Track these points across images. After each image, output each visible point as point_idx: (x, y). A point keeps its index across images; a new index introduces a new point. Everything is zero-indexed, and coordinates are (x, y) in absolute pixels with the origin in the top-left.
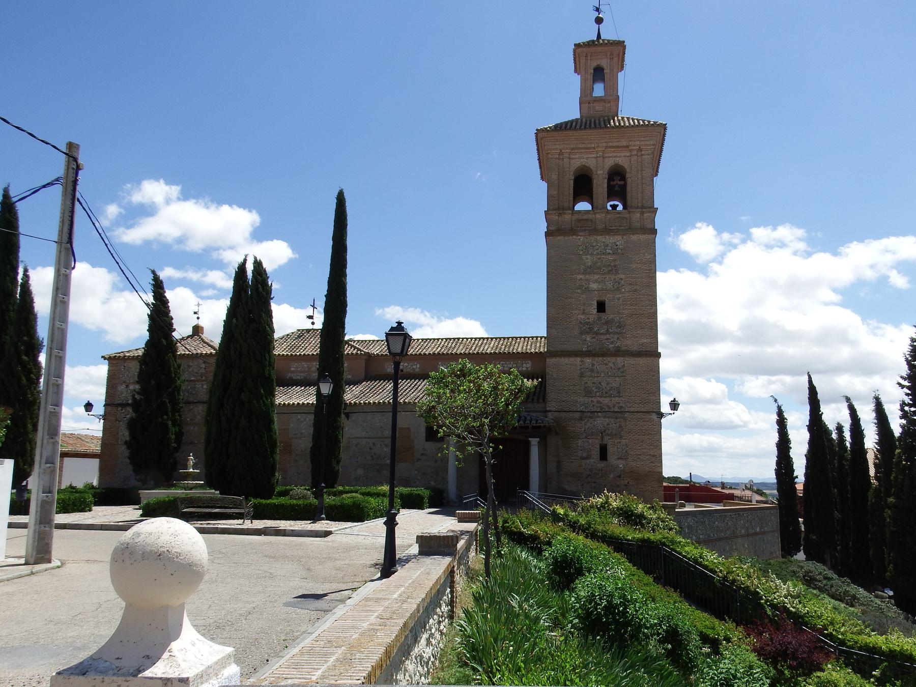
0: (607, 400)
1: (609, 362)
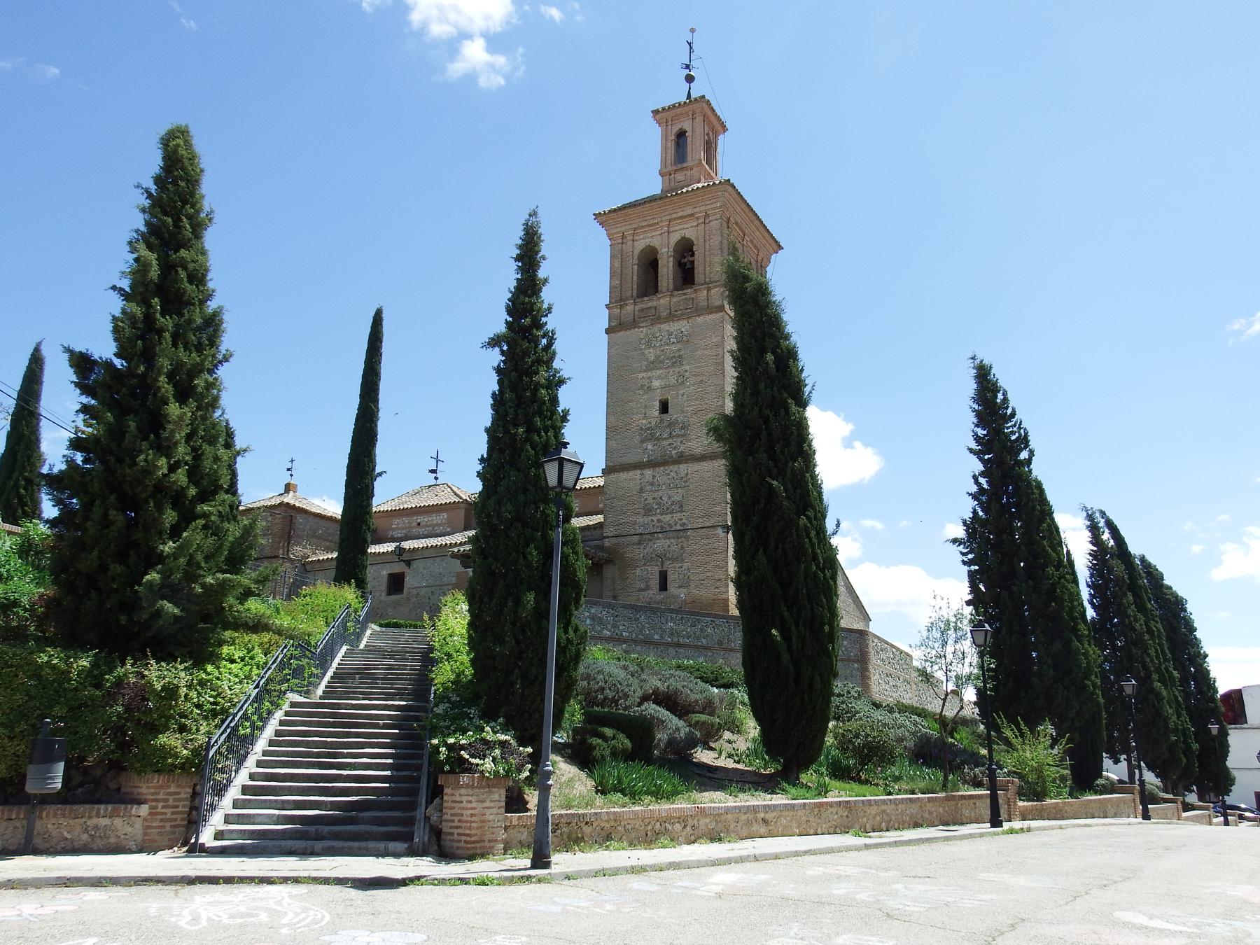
0: (667, 518)
1: (671, 471)
